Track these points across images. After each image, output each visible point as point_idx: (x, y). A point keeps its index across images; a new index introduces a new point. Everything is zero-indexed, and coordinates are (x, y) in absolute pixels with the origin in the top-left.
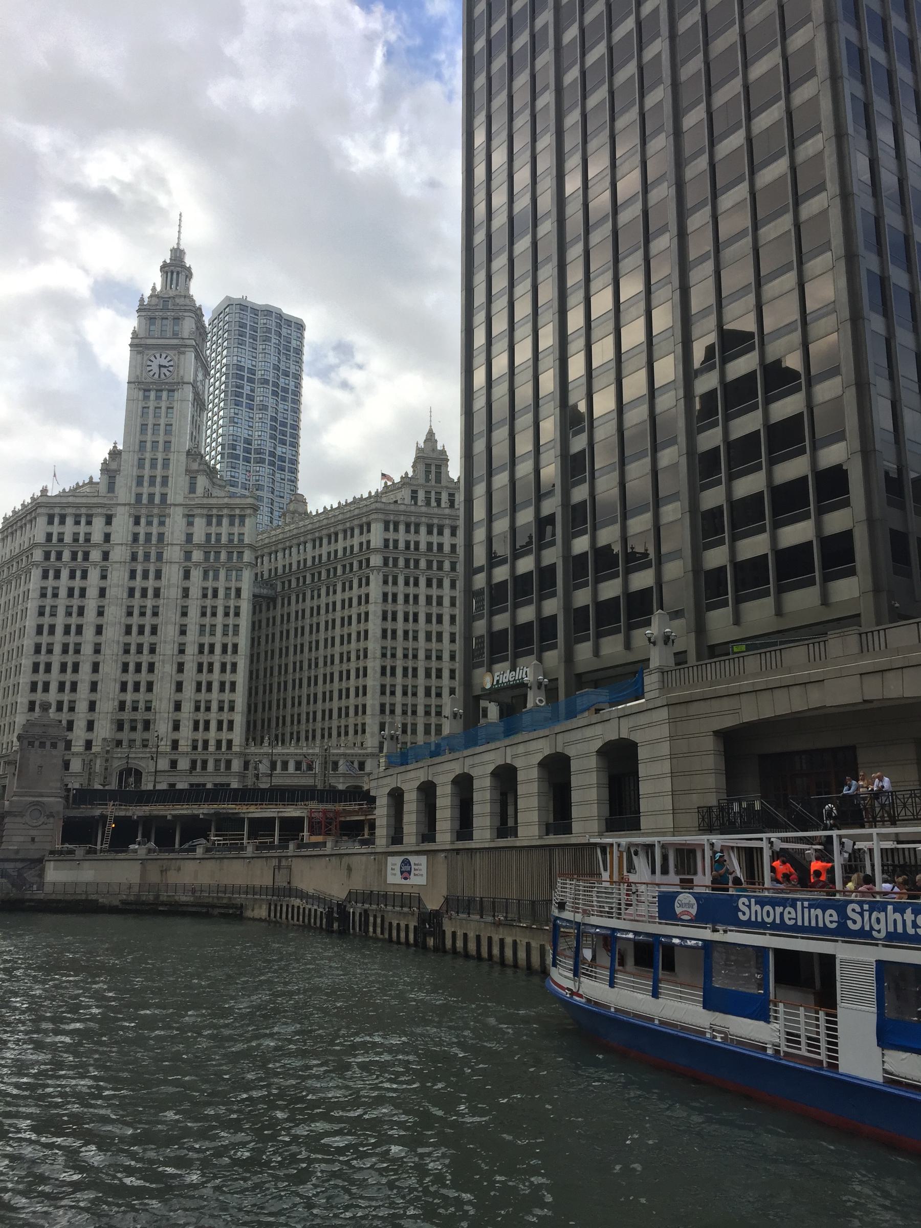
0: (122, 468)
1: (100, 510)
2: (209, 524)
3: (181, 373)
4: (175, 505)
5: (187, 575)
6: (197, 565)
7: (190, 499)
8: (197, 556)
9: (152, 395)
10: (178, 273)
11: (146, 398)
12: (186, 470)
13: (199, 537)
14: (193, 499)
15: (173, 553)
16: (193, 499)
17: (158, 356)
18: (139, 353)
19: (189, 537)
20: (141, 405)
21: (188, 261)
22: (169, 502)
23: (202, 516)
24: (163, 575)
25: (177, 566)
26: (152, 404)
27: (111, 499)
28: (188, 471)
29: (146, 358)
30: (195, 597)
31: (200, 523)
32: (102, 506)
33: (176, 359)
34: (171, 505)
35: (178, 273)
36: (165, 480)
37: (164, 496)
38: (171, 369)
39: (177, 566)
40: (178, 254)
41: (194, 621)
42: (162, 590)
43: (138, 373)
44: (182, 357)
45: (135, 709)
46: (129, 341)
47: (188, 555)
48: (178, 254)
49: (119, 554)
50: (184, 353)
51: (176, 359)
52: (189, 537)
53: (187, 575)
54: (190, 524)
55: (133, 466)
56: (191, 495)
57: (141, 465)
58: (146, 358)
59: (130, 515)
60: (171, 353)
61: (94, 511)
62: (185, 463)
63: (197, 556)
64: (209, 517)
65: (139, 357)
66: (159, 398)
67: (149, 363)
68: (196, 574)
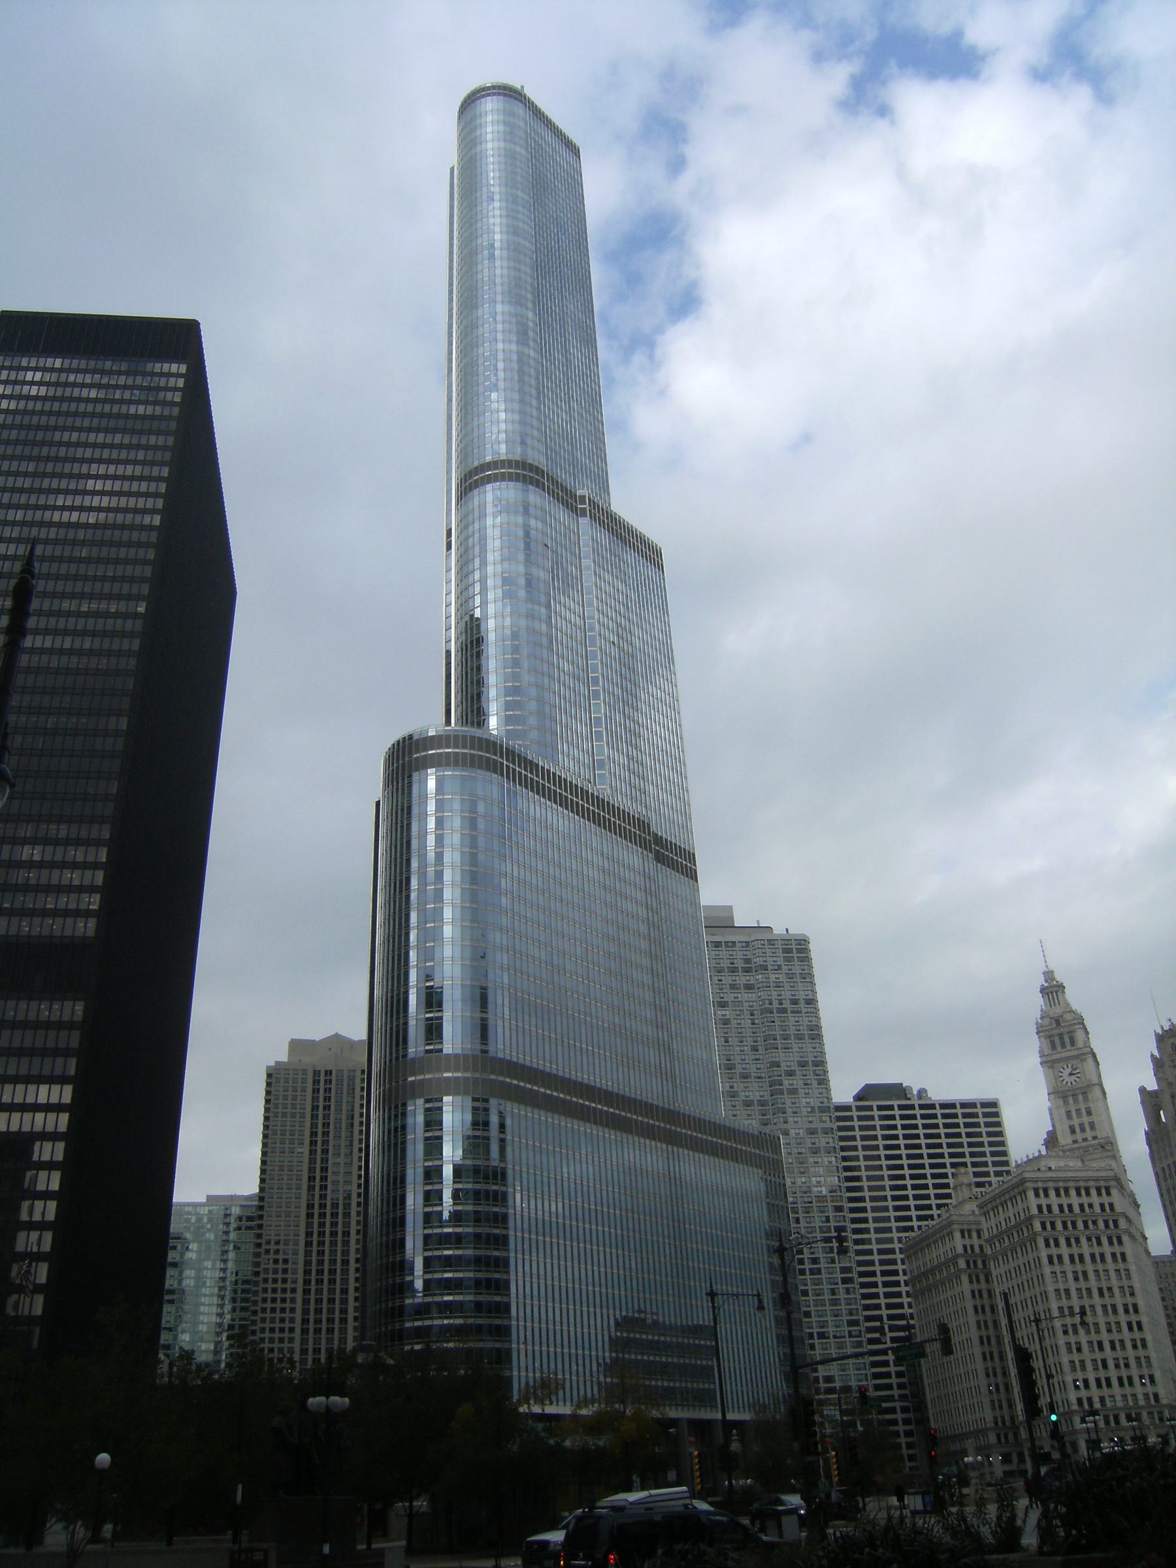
9: (1071, 1100)
10: (1056, 992)
11: (1066, 1102)
20: (1063, 1111)
21: (1059, 977)
26: (1073, 1109)
29: (1056, 1071)
33: (1080, 1066)
35: (1056, 992)
38: (1079, 1075)
40: (1049, 975)
44: (1085, 1064)
46: (1039, 1060)
48: (1049, 975)
50: (1085, 1060)
58: (1056, 1071)
60: (1074, 1062)
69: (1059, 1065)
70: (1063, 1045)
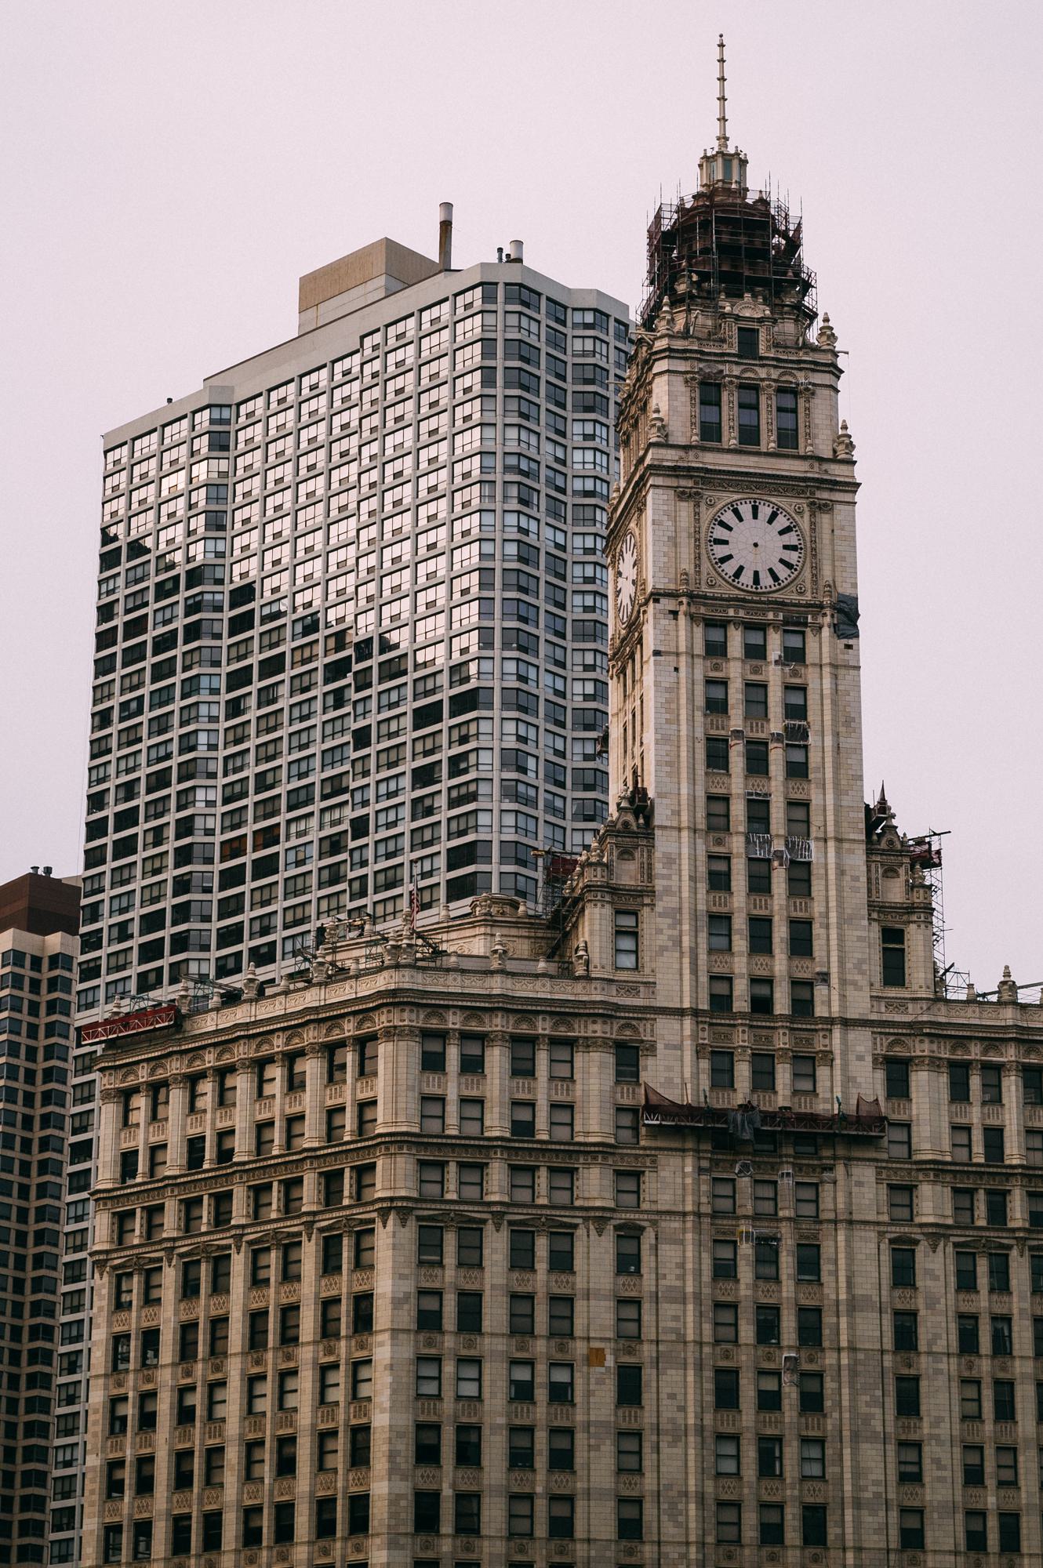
0: (659, 884)
1: (597, 1029)
2: (959, 1093)
4: (846, 1023)
5: (903, 1273)
6: (937, 1234)
7: (890, 1003)
11: (716, 651)
12: (871, 906)
14: (900, 1004)
16: (900, 1004)
17: (745, 510)
18: (682, 495)
22: (820, 1011)
23: (934, 1063)
24: (826, 1267)
25: (872, 1234)
26: (735, 671)
27: (632, 988)
28: (877, 908)
29: (707, 515)
30: (940, 1346)
32: (608, 1013)
34: (831, 1021)
36: (801, 941)
37: (803, 992)
39: (872, 1234)
41: (944, 1430)
42: (828, 1319)
43: (687, 565)
44: (824, 520)
50: (826, 507)
51: (805, 523)
53: (903, 1273)
55: (693, 879)
56: (893, 992)
57: (719, 881)
58: (707, 515)
59: (699, 1052)
61: (579, 1030)
62: (864, 879)
64: (958, 1074)
65: (685, 509)
66: (755, 653)
67: (720, 533)
70: (749, 436)
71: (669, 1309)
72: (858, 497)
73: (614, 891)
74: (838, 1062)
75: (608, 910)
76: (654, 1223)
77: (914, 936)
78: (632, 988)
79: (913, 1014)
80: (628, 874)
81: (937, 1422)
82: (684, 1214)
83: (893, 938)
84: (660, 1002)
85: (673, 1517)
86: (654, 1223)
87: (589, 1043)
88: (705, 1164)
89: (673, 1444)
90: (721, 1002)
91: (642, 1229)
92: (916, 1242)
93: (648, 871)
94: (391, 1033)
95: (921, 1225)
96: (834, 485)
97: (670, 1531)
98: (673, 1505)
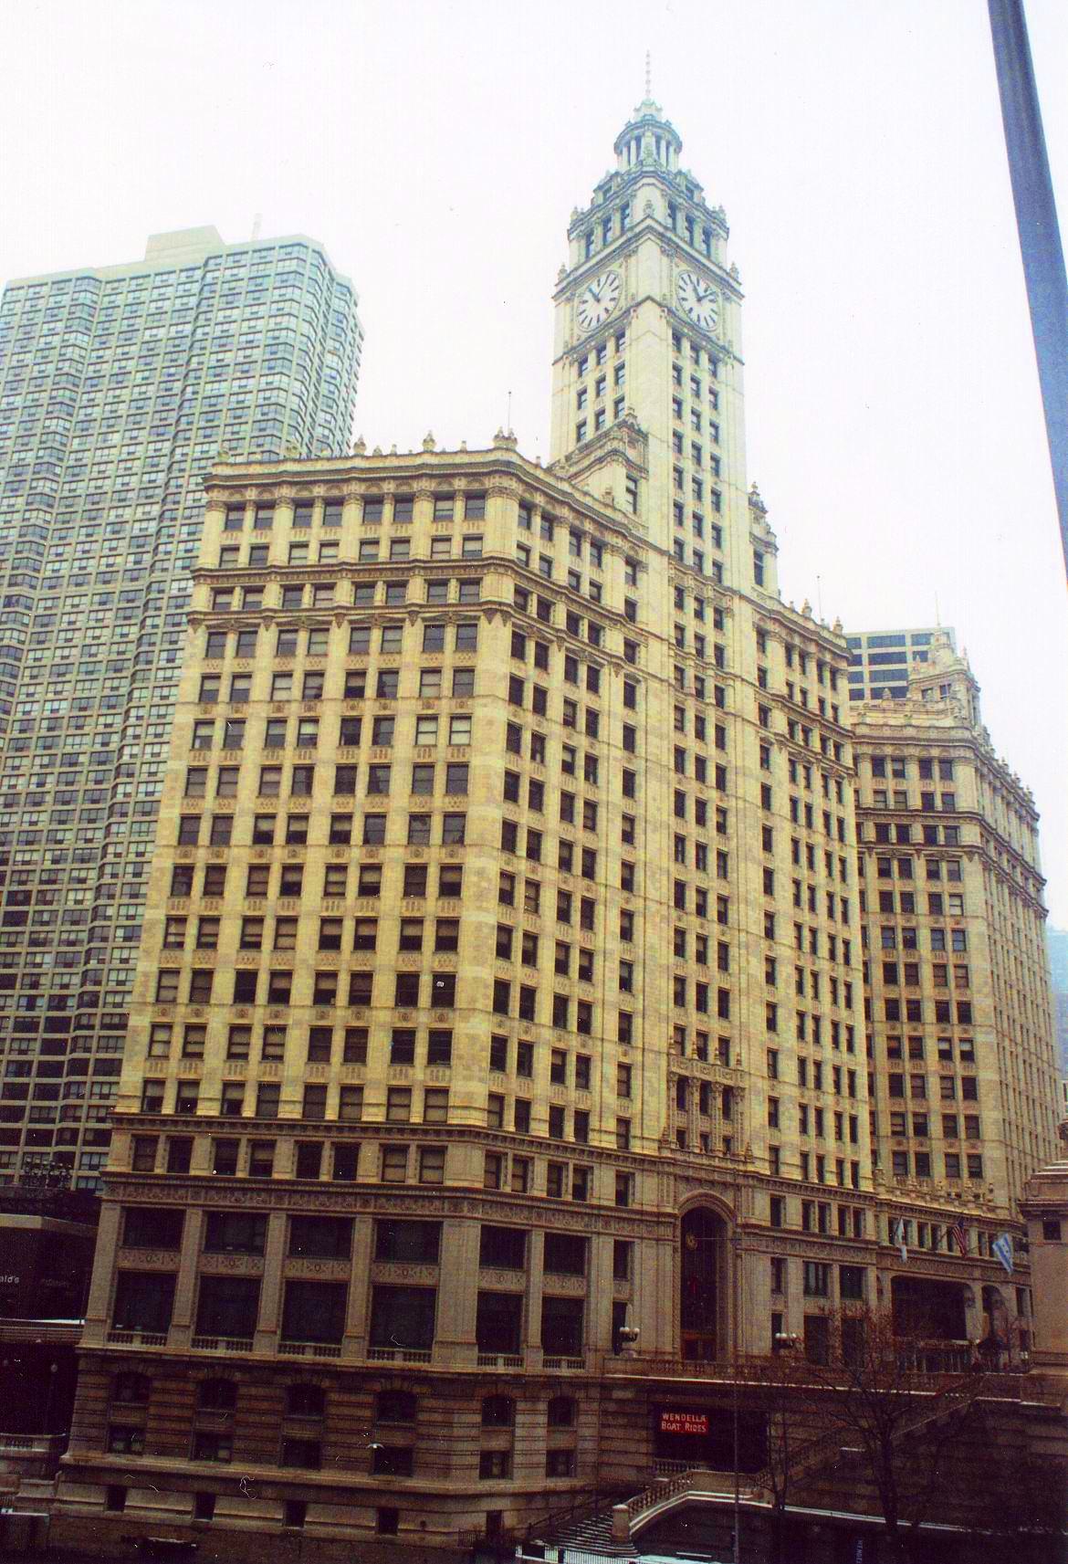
3: (729, 337)
4: (742, 597)
5: (765, 761)
8: (779, 721)
13: (777, 683)
15: (743, 699)
16: (760, 595)
18: (663, 252)
19: (762, 673)
29: (676, 271)
31: (776, 650)
34: (734, 592)
43: (666, 291)
45: (702, 1053)
47: (764, 712)
49: (656, 659)
50: (728, 299)
52: (762, 673)
53: (765, 761)
54: (762, 646)
63: (779, 721)
64: (789, 649)
65: (665, 260)
68: (780, 759)
69: (684, 267)
71: (653, 740)
72: (742, 302)
73: (628, 460)
74: (737, 618)
75: (624, 471)
76: (646, 680)
77: (768, 559)
78: (636, 525)
79: (770, 605)
80: (631, 454)
81: (782, 860)
82: (662, 680)
83: (758, 556)
84: (650, 540)
85: (653, 883)
86: (646, 680)
87: (615, 550)
88: (672, 653)
89: (654, 831)
90: (680, 555)
91: (638, 681)
92: (771, 744)
93: (644, 457)
94: (502, 491)
95: (776, 734)
96: (735, 291)
97: (652, 894)
98: (654, 874)
